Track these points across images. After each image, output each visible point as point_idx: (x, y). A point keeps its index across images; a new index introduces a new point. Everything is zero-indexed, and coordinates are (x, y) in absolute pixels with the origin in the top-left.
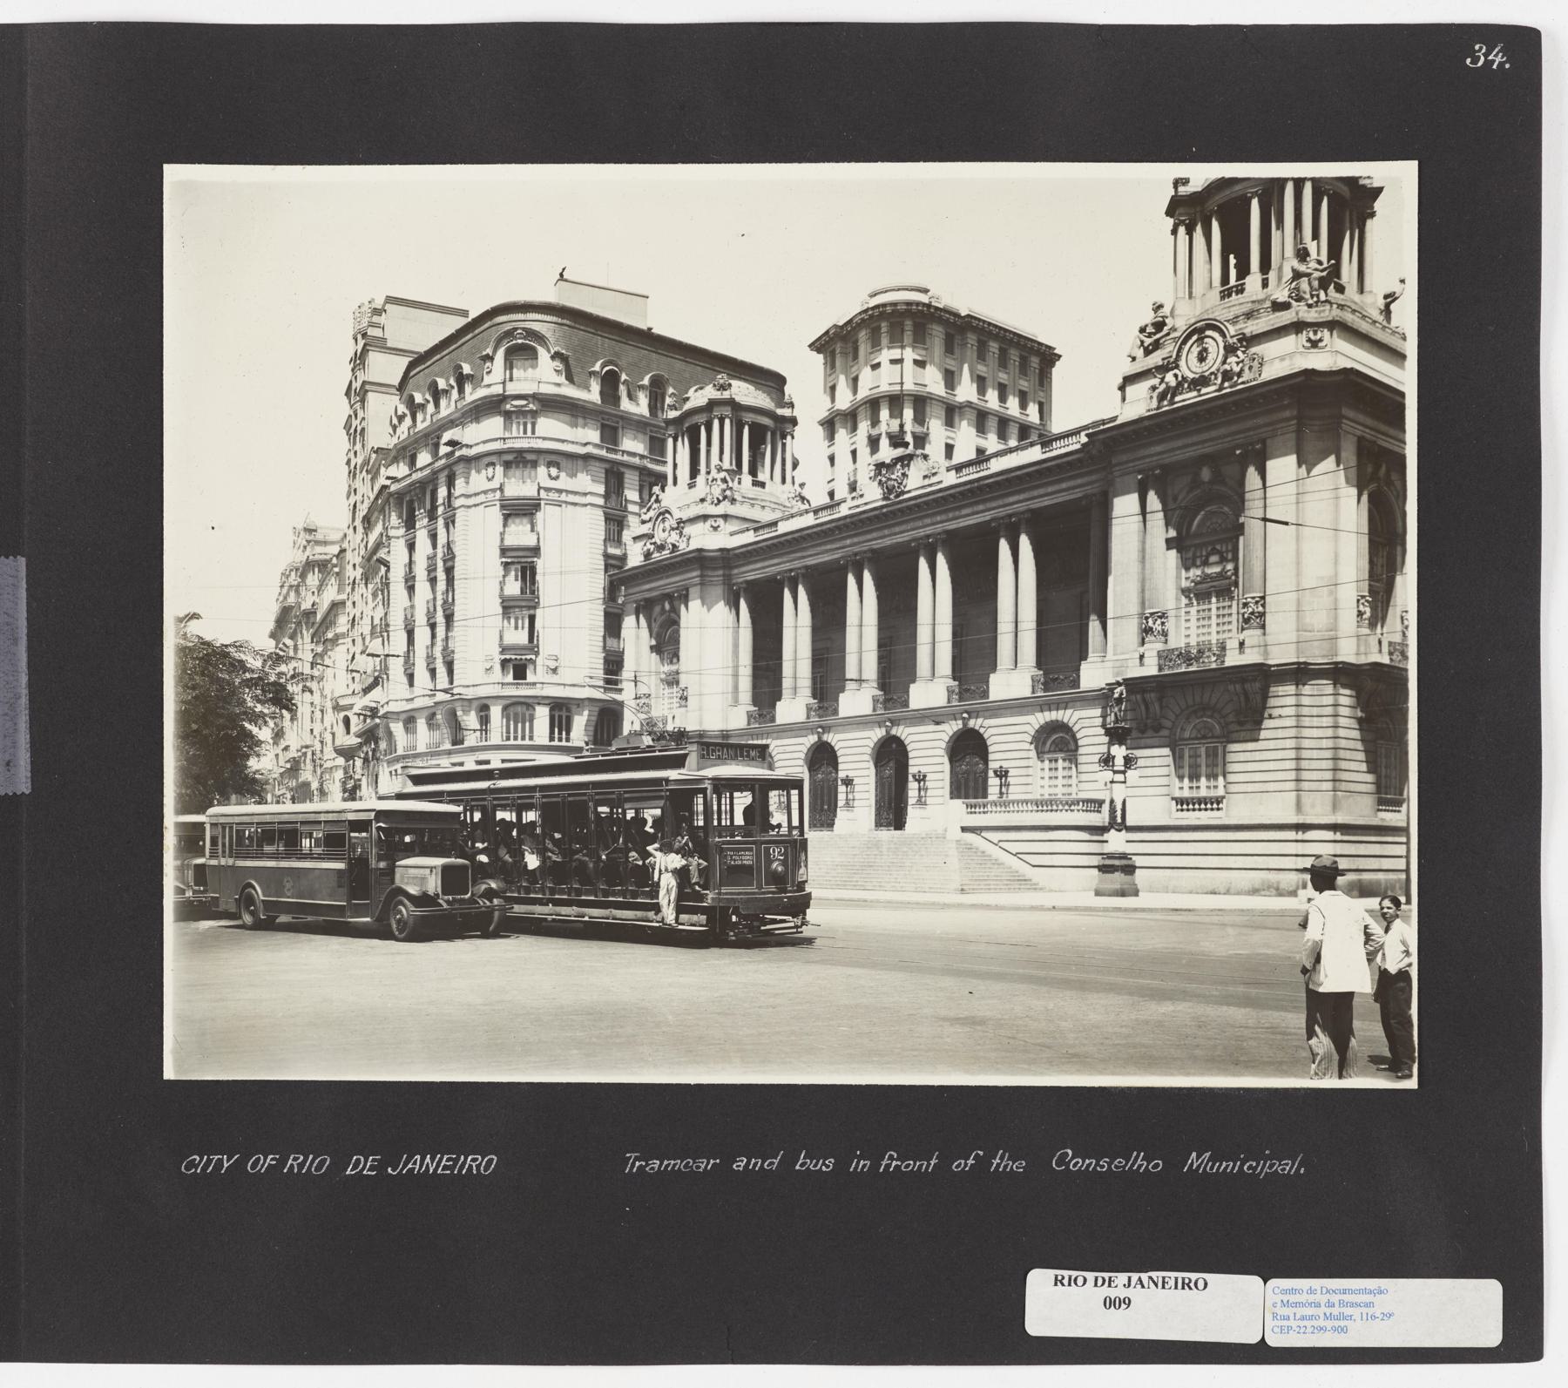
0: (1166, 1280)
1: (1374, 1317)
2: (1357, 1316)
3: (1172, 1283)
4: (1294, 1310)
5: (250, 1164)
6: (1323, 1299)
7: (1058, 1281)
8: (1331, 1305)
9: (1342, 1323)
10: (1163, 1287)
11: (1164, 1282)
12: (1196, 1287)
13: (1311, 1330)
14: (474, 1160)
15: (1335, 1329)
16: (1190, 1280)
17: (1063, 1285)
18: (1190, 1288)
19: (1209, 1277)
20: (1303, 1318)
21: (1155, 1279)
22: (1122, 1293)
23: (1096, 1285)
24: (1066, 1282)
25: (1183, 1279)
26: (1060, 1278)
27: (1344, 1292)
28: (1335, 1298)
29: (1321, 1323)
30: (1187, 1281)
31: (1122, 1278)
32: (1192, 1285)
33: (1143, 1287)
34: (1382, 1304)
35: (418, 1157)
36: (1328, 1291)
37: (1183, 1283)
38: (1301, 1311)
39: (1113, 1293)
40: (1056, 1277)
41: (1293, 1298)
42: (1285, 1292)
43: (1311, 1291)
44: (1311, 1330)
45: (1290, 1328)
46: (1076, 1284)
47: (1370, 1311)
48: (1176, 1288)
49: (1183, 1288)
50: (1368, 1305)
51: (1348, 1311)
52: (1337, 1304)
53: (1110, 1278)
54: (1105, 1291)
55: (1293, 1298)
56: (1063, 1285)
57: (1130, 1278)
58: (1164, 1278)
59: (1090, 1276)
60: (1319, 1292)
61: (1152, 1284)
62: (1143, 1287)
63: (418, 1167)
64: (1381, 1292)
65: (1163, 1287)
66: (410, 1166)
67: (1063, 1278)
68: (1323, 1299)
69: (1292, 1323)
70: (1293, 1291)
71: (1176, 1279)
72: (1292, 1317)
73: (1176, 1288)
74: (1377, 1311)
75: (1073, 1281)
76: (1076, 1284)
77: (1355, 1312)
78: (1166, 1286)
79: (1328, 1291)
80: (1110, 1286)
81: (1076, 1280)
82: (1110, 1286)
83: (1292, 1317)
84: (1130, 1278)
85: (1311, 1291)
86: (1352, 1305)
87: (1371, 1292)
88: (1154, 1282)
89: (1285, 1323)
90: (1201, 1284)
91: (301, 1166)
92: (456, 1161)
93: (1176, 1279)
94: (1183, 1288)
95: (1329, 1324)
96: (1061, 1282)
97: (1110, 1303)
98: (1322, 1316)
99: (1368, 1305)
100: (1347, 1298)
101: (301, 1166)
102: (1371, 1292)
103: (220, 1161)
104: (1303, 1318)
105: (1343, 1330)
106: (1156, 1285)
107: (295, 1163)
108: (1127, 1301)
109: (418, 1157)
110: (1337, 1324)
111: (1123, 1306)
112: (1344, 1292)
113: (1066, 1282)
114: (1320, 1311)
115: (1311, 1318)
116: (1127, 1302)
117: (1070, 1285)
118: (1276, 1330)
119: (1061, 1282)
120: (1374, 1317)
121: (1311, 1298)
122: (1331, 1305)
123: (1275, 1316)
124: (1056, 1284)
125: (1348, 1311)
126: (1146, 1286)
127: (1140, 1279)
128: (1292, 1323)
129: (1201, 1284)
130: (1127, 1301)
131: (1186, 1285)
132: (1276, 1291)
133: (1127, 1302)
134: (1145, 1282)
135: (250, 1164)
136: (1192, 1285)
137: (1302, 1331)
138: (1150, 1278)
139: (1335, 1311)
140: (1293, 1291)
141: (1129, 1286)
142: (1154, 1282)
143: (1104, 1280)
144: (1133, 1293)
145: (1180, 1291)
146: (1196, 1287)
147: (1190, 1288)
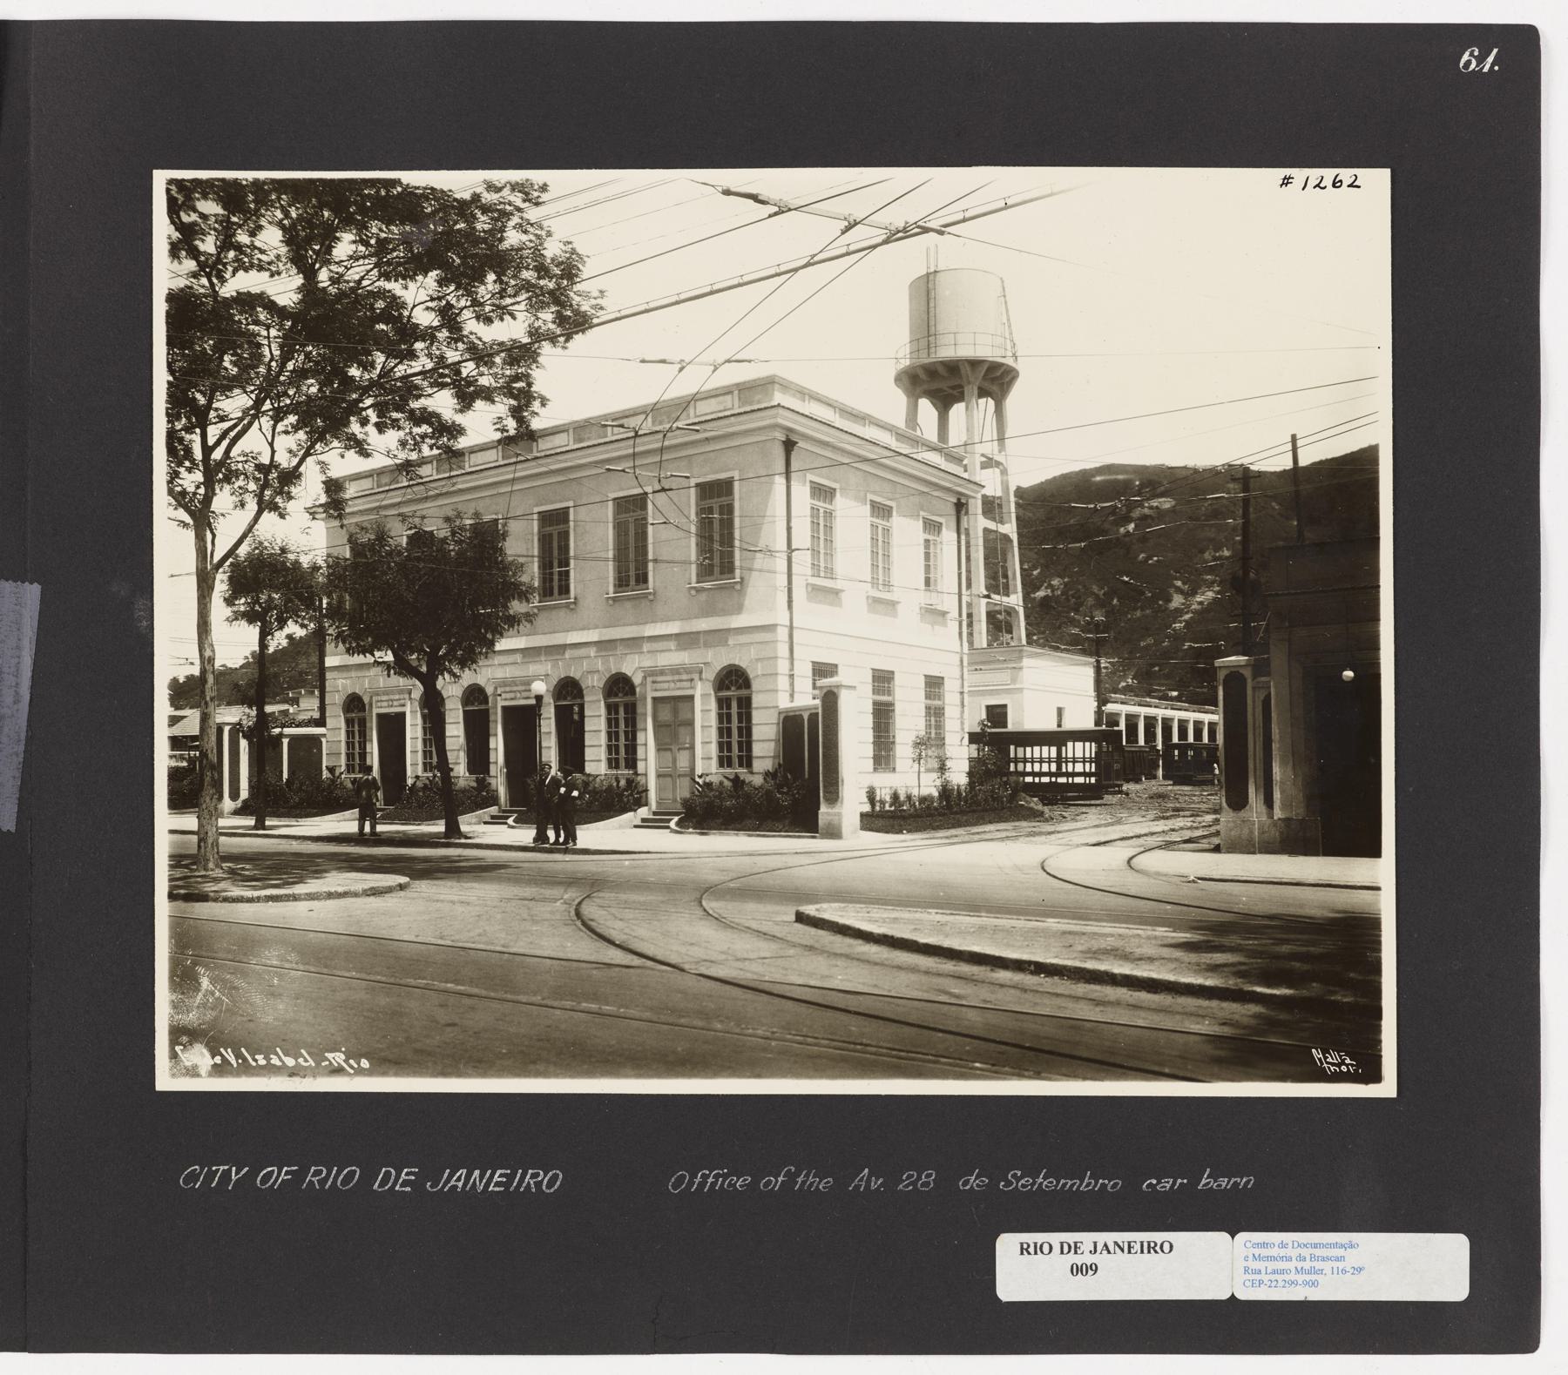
0: (1132, 1244)
1: (1344, 1271)
2: (1328, 1271)
3: (1137, 1247)
4: (1266, 1264)
5: (259, 1178)
6: (1294, 1253)
7: (1024, 1249)
8: (1301, 1258)
9: (1313, 1277)
10: (1129, 1252)
11: (1129, 1247)
12: (1163, 1251)
13: (1282, 1284)
14: (534, 1176)
15: (1306, 1283)
16: (1156, 1245)
17: (1029, 1253)
18: (1156, 1252)
19: (1180, 1238)
20: (1274, 1272)
21: (1121, 1244)
22: (1088, 1259)
23: (1062, 1253)
24: (1032, 1250)
25: (1149, 1243)
26: (1025, 1246)
27: (1315, 1246)
28: (1306, 1252)
29: (1292, 1277)
30: (1152, 1245)
31: (1087, 1238)
32: (1158, 1248)
33: (1109, 1252)
34: (1352, 1258)
35: (464, 1171)
36: (1299, 1246)
37: (1149, 1245)
38: (1271, 1266)
39: (1079, 1260)
40: (1022, 1244)
41: (1265, 1252)
42: (1258, 1245)
43: (1283, 1245)
44: (1282, 1284)
45: (1261, 1282)
46: (1042, 1252)
47: (1341, 1265)
48: (1142, 1252)
49: (1149, 1252)
50: (1338, 1259)
51: (1318, 1265)
52: (1308, 1258)
53: (1076, 1243)
54: (1072, 1258)
55: (1265, 1252)
56: (1029, 1253)
57: (1095, 1243)
58: (1129, 1243)
59: (1055, 1238)
60: (1290, 1245)
61: (1117, 1248)
62: (1109, 1252)
63: (460, 1184)
64: (1352, 1246)
65: (1129, 1252)
66: (452, 1183)
67: (1029, 1246)
68: (1294, 1253)
69: (1265, 1278)
70: (1264, 1245)
71: (1142, 1243)
72: (1263, 1271)
73: (1142, 1252)
74: (1347, 1265)
75: (1038, 1249)
76: (1042, 1252)
77: (1327, 1266)
78: (1132, 1251)
79: (1299, 1246)
80: (1076, 1253)
81: (1041, 1246)
82: (1076, 1253)
83: (1263, 1271)
84: (1095, 1243)
85: (1283, 1245)
86: (1323, 1259)
87: (1342, 1246)
88: (1119, 1246)
89: (1257, 1277)
90: (1166, 1247)
91: (323, 1182)
92: (511, 1177)
93: (1142, 1243)
94: (1149, 1252)
95: (1300, 1278)
96: (1027, 1250)
97: (1077, 1270)
98: (1293, 1271)
99: (1338, 1259)
100: (1318, 1252)
101: (323, 1182)
102: (1342, 1246)
103: (227, 1174)
104: (1274, 1272)
105: (1314, 1284)
106: (1122, 1250)
107: (315, 1179)
108: (1094, 1267)
109: (464, 1171)
110: (1308, 1277)
111: (1090, 1272)
112: (1315, 1246)
113: (1032, 1250)
114: (1291, 1265)
115: (1283, 1272)
116: (1094, 1268)
117: (1036, 1253)
118: (1248, 1283)
119: (1027, 1250)
120: (1344, 1271)
121: (1283, 1252)
122: (1301, 1258)
123: (1246, 1270)
124: (1022, 1253)
125: (1318, 1265)
126: (1112, 1251)
127: (1106, 1245)
128: (1265, 1278)
129: (1166, 1247)
130: (1094, 1267)
131: (1151, 1248)
132: (1248, 1245)
133: (1094, 1268)
134: (1111, 1248)
135: (259, 1178)
136: (1158, 1248)
137: (1273, 1284)
138: (1116, 1243)
139: (1307, 1265)
140: (1264, 1245)
141: (1095, 1251)
142: (1119, 1246)
143: (1070, 1247)
144: (1100, 1259)
145: (1146, 1255)
146: (1163, 1251)
147: (1156, 1252)
